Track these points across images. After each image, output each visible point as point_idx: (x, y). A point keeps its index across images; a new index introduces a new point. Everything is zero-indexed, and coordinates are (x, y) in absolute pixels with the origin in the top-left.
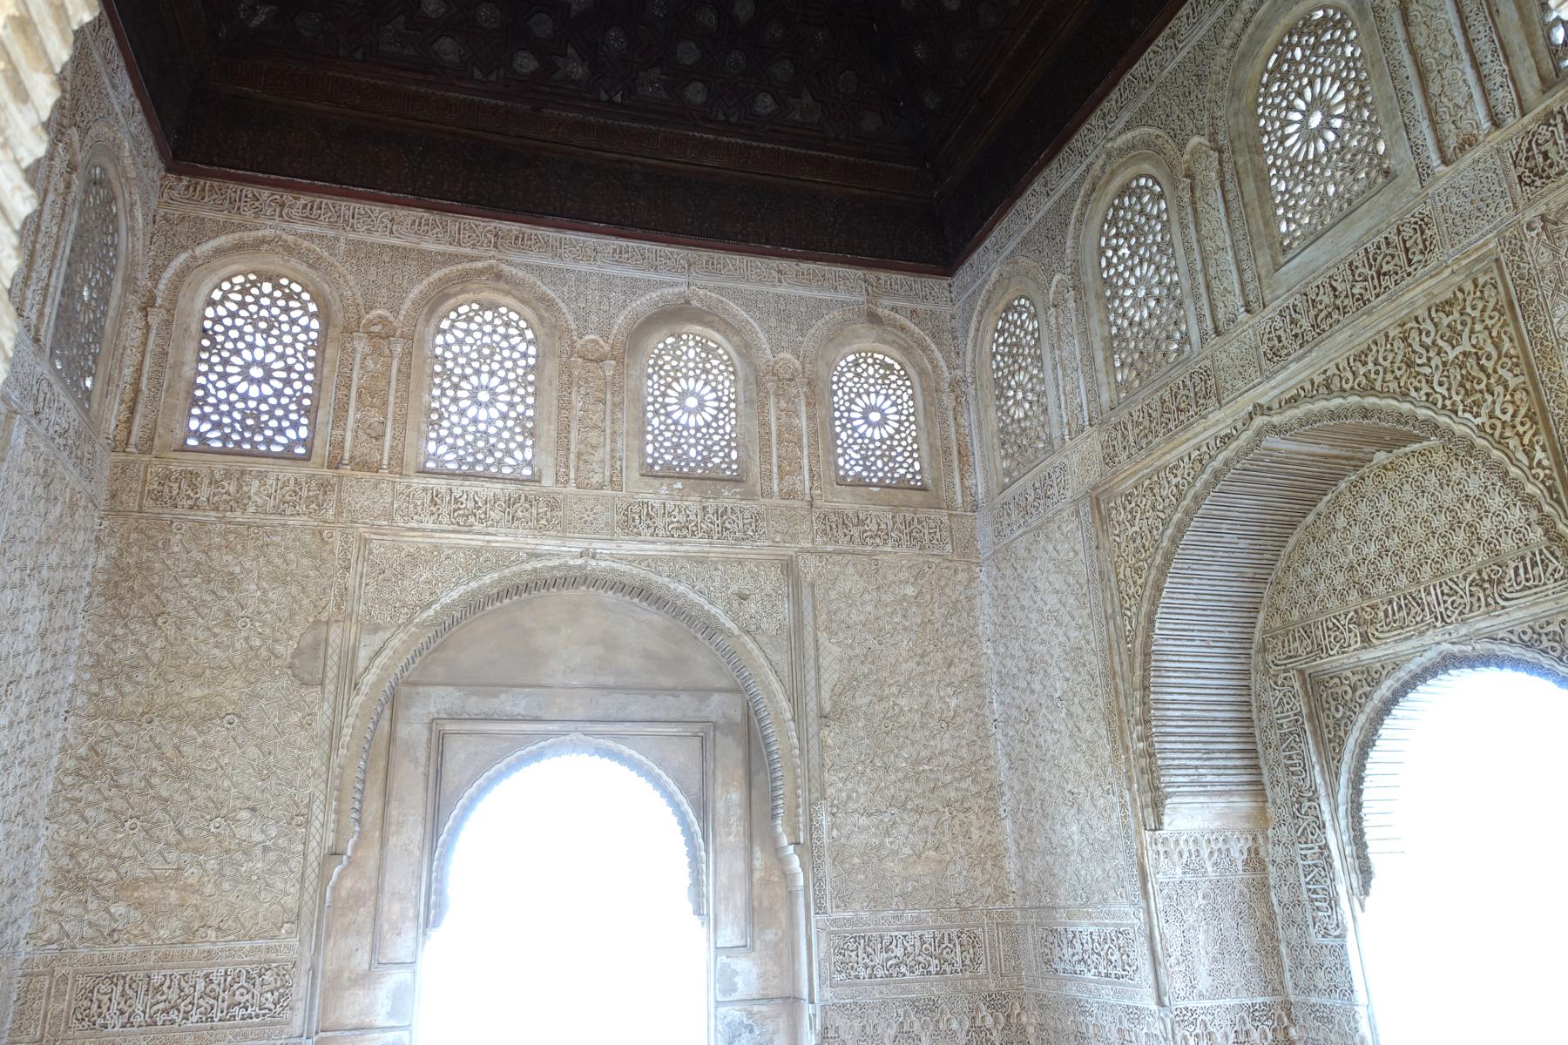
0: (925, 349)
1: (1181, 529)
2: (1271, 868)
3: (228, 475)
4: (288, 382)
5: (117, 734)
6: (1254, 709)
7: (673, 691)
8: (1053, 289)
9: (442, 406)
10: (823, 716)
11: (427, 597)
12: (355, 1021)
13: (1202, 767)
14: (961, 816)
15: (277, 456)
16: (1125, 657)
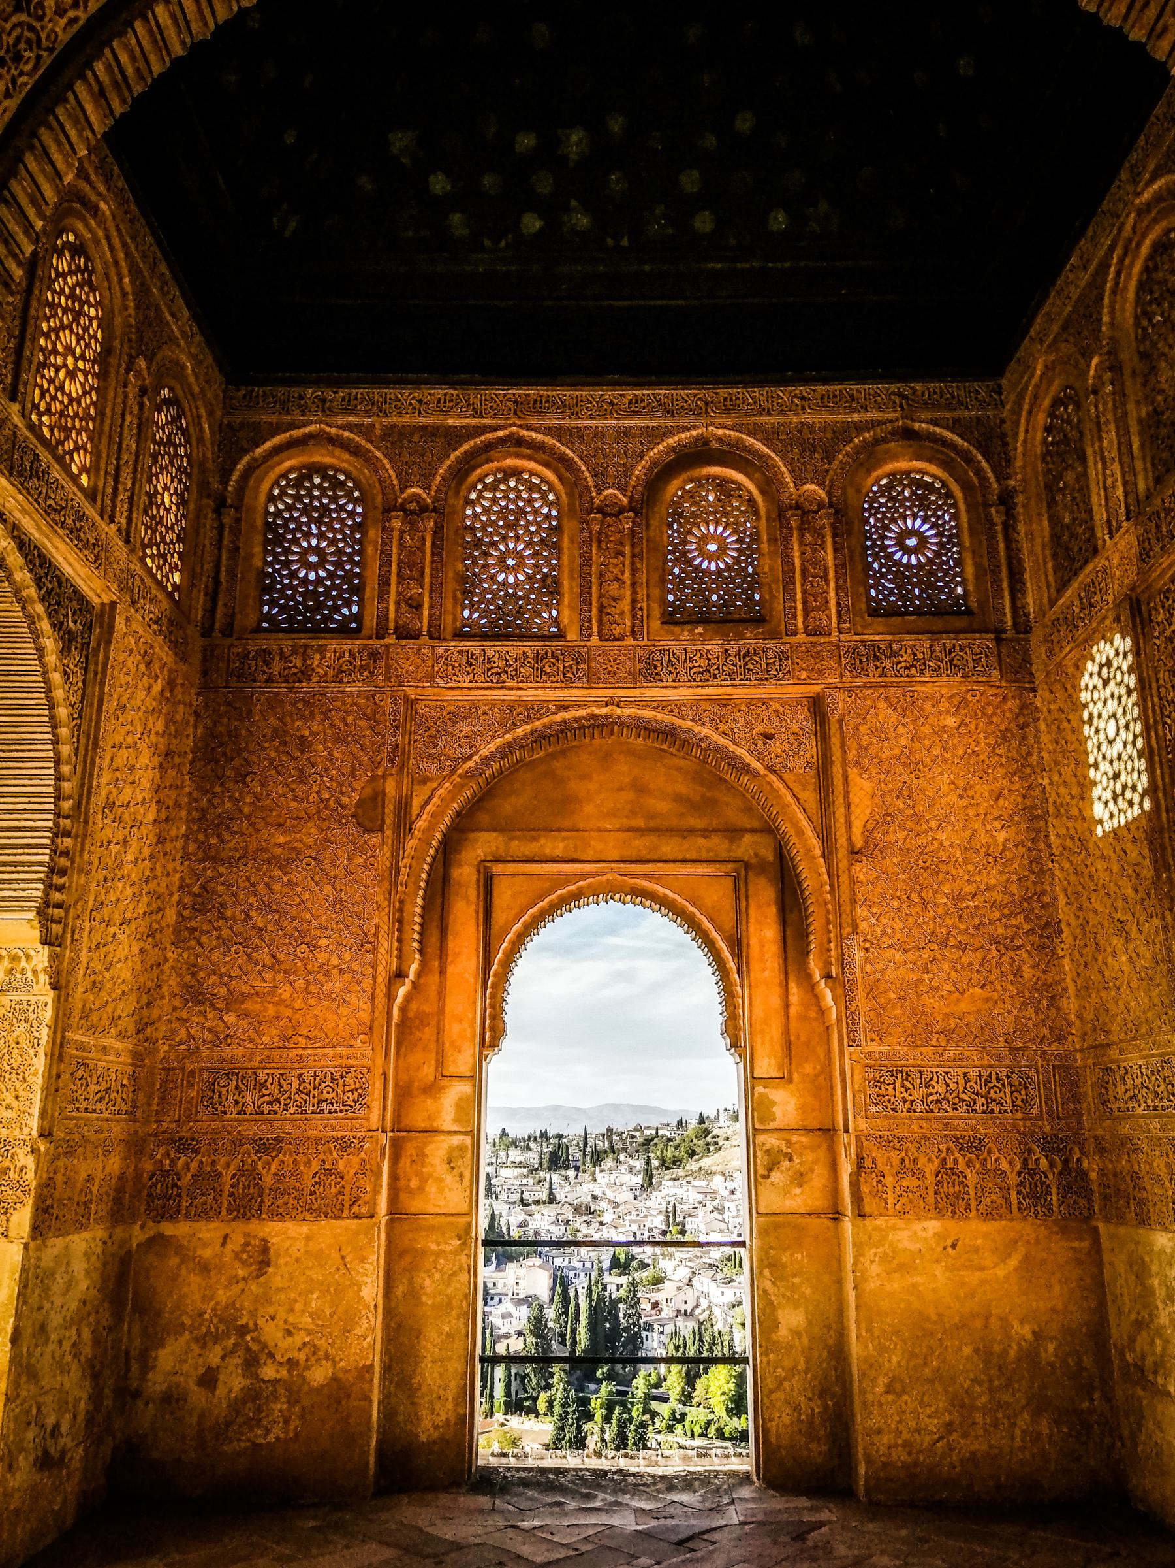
0: (969, 460)
3: (294, 652)
4: (339, 565)
5: (221, 875)
7: (706, 833)
9: (475, 574)
10: (853, 852)
11: (467, 750)
12: (423, 1125)
14: (1011, 954)
15: (333, 631)
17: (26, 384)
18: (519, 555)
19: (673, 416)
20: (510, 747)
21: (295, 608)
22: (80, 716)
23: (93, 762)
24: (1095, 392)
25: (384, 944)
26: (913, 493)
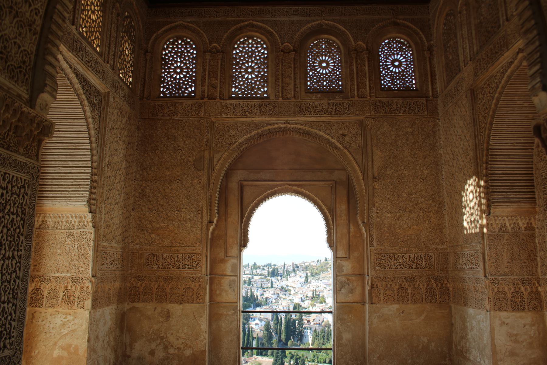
1: (498, 100)
2: (537, 230)
3: (172, 105)
6: (534, 170)
8: (459, 6)
9: (236, 75)
10: (374, 178)
11: (234, 141)
12: (221, 273)
13: (509, 192)
16: (481, 151)
17: (77, 18)
18: (252, 68)
19: (310, 16)
20: (248, 140)
21: (172, 88)
22: (99, 133)
23: (103, 149)
24: (460, 13)
25: (205, 211)
26: (397, 45)
